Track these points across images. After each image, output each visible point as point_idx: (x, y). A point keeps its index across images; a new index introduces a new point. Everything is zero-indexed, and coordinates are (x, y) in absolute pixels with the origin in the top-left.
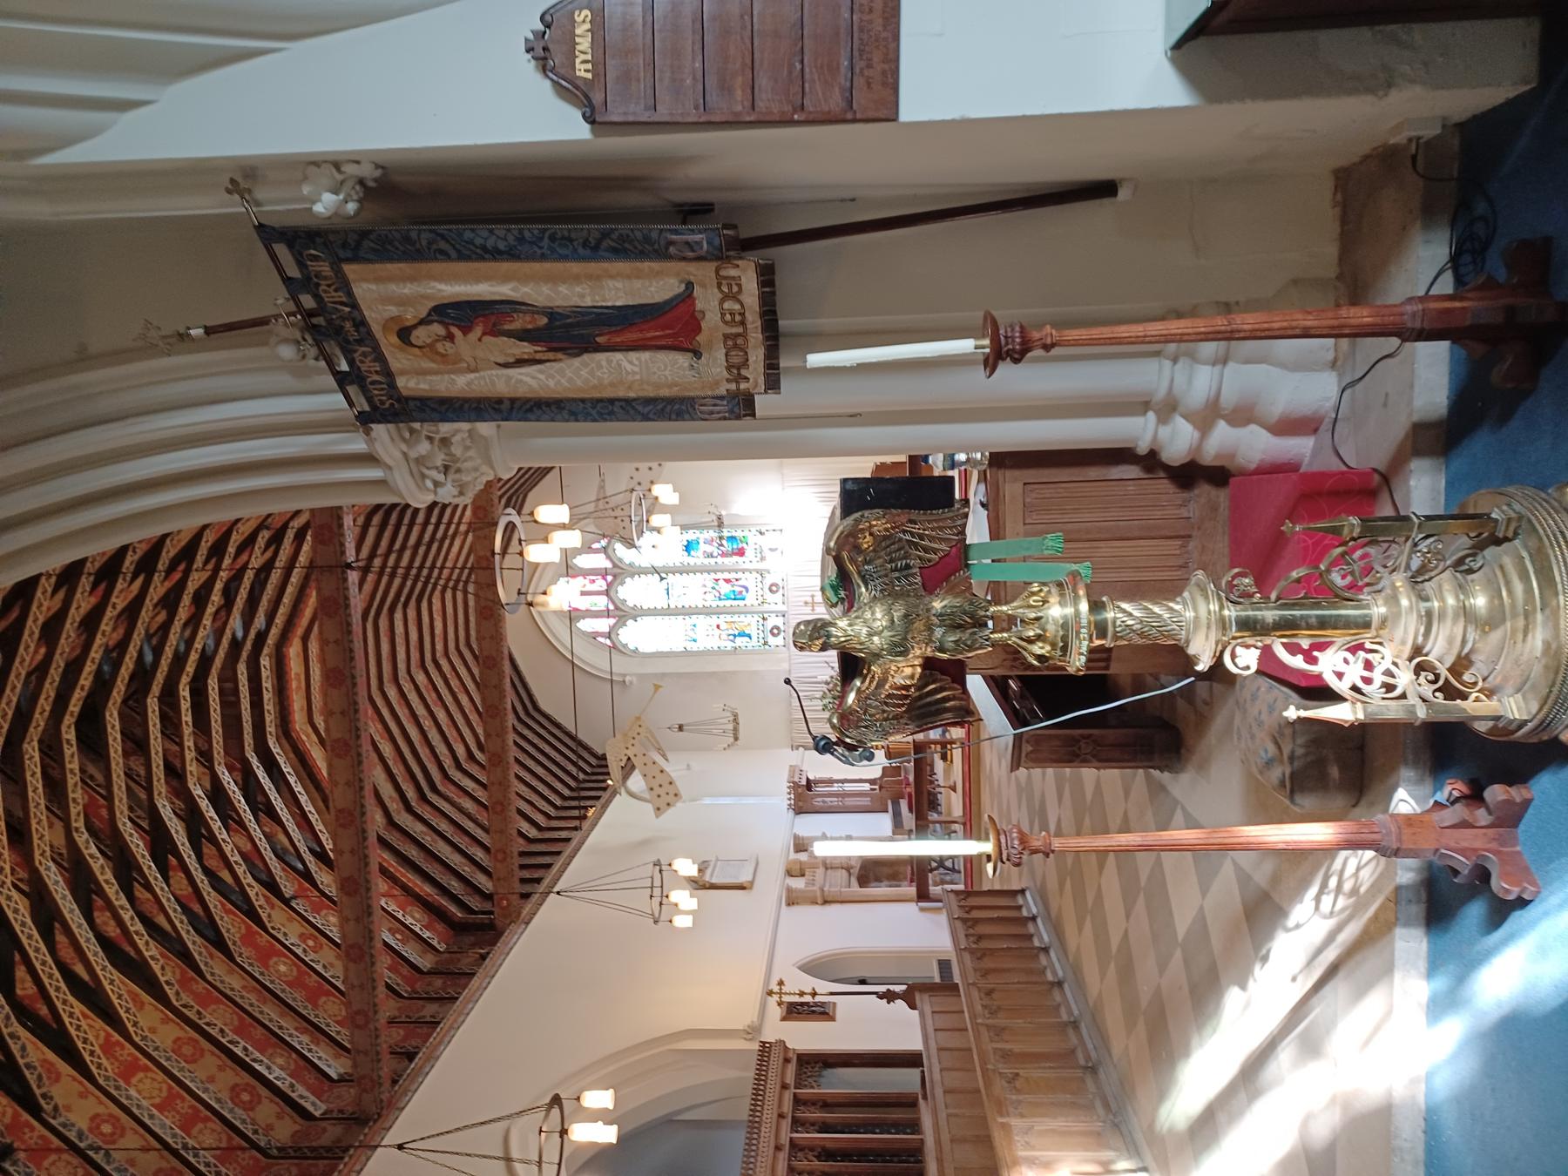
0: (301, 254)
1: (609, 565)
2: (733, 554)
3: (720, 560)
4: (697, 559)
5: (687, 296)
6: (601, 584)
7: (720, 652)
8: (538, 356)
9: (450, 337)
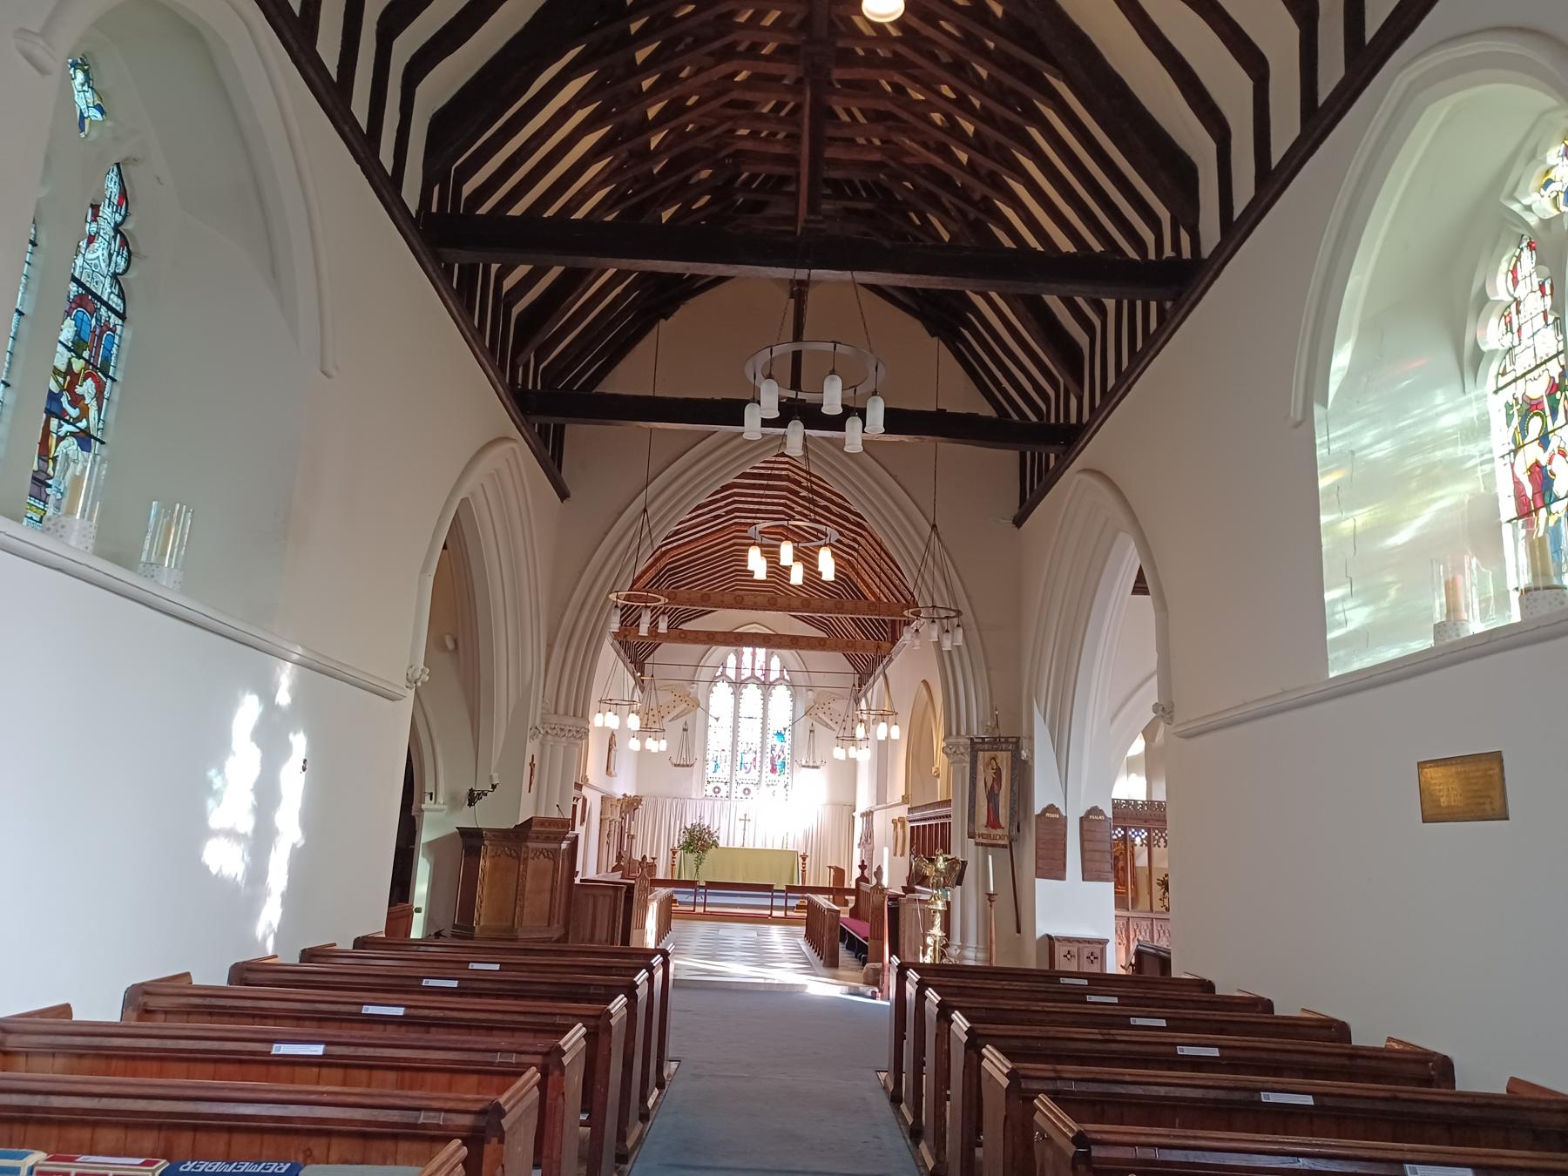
1: (772, 679)
4: (772, 740)
6: (759, 673)
7: (705, 750)
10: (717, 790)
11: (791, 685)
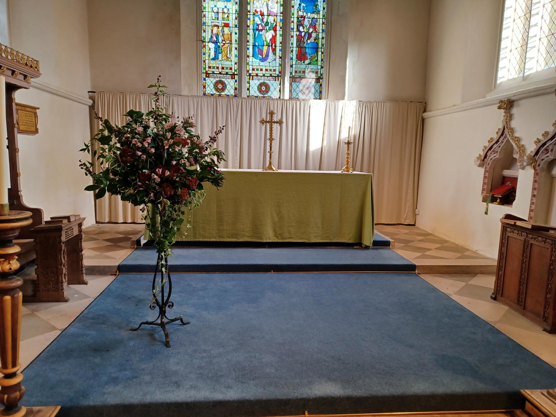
2: (299, 46)
3: (295, 33)
7: (199, 25)
10: (220, 86)
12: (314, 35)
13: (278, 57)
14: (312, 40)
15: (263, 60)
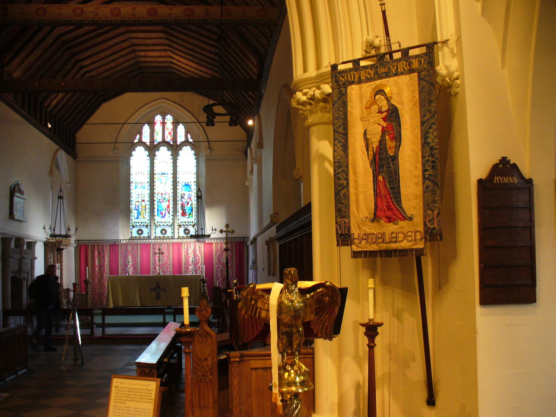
0: (422, 57)
5: (404, 217)
6: (168, 138)
8: (370, 149)
9: (380, 112)
11: (194, 146)
12: (190, 203)
13: (171, 215)
14: (189, 205)
15: (163, 217)
